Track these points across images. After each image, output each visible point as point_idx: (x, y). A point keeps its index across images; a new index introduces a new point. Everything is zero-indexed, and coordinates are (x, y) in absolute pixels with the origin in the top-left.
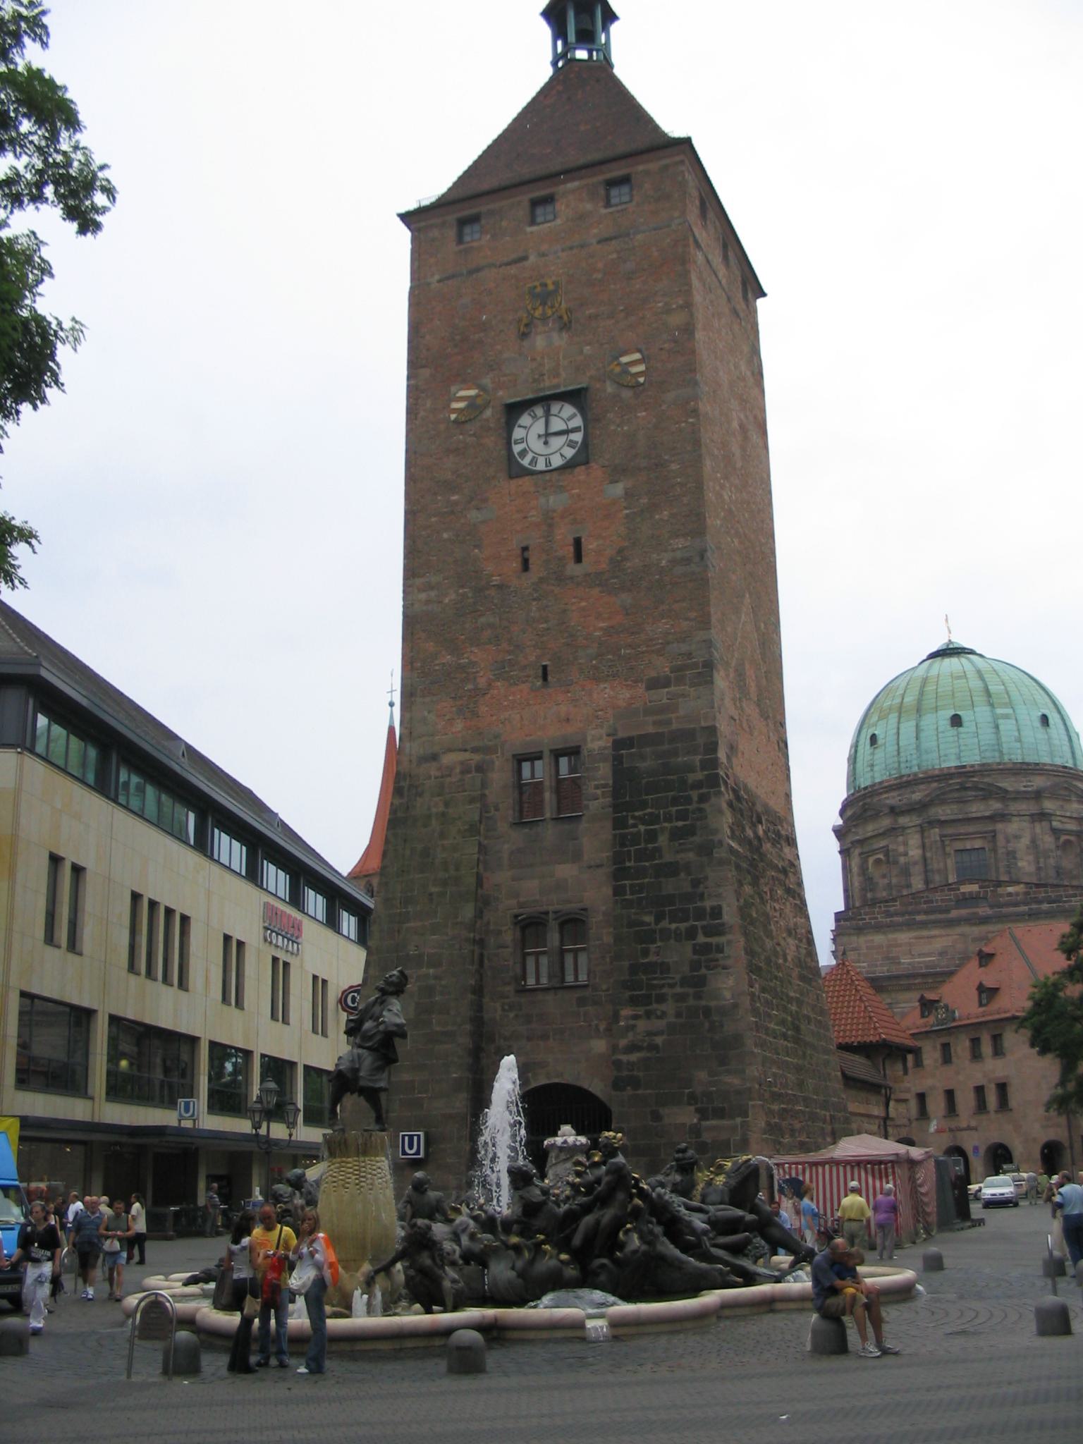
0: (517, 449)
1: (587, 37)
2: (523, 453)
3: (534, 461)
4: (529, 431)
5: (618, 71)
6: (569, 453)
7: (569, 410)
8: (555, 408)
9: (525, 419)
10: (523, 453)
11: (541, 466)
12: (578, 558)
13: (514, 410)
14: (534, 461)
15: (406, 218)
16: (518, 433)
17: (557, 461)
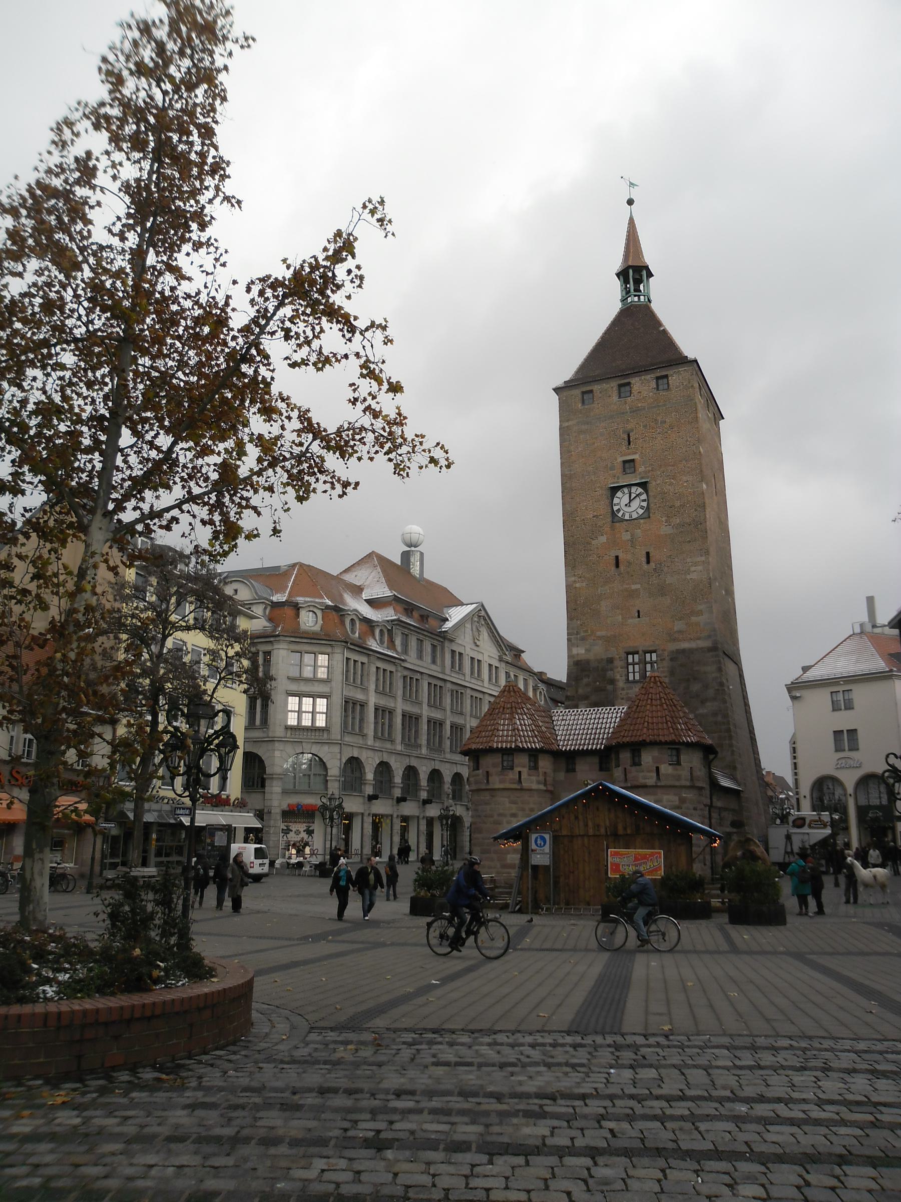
0: (615, 508)
1: (637, 290)
2: (619, 510)
3: (623, 515)
4: (621, 499)
5: (653, 306)
6: (641, 511)
7: (640, 490)
8: (634, 489)
9: (619, 494)
10: (619, 510)
11: (627, 517)
12: (648, 562)
13: (614, 490)
14: (623, 515)
15: (556, 390)
16: (616, 501)
17: (635, 516)
